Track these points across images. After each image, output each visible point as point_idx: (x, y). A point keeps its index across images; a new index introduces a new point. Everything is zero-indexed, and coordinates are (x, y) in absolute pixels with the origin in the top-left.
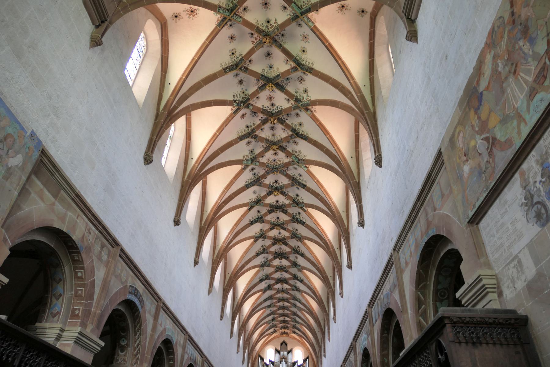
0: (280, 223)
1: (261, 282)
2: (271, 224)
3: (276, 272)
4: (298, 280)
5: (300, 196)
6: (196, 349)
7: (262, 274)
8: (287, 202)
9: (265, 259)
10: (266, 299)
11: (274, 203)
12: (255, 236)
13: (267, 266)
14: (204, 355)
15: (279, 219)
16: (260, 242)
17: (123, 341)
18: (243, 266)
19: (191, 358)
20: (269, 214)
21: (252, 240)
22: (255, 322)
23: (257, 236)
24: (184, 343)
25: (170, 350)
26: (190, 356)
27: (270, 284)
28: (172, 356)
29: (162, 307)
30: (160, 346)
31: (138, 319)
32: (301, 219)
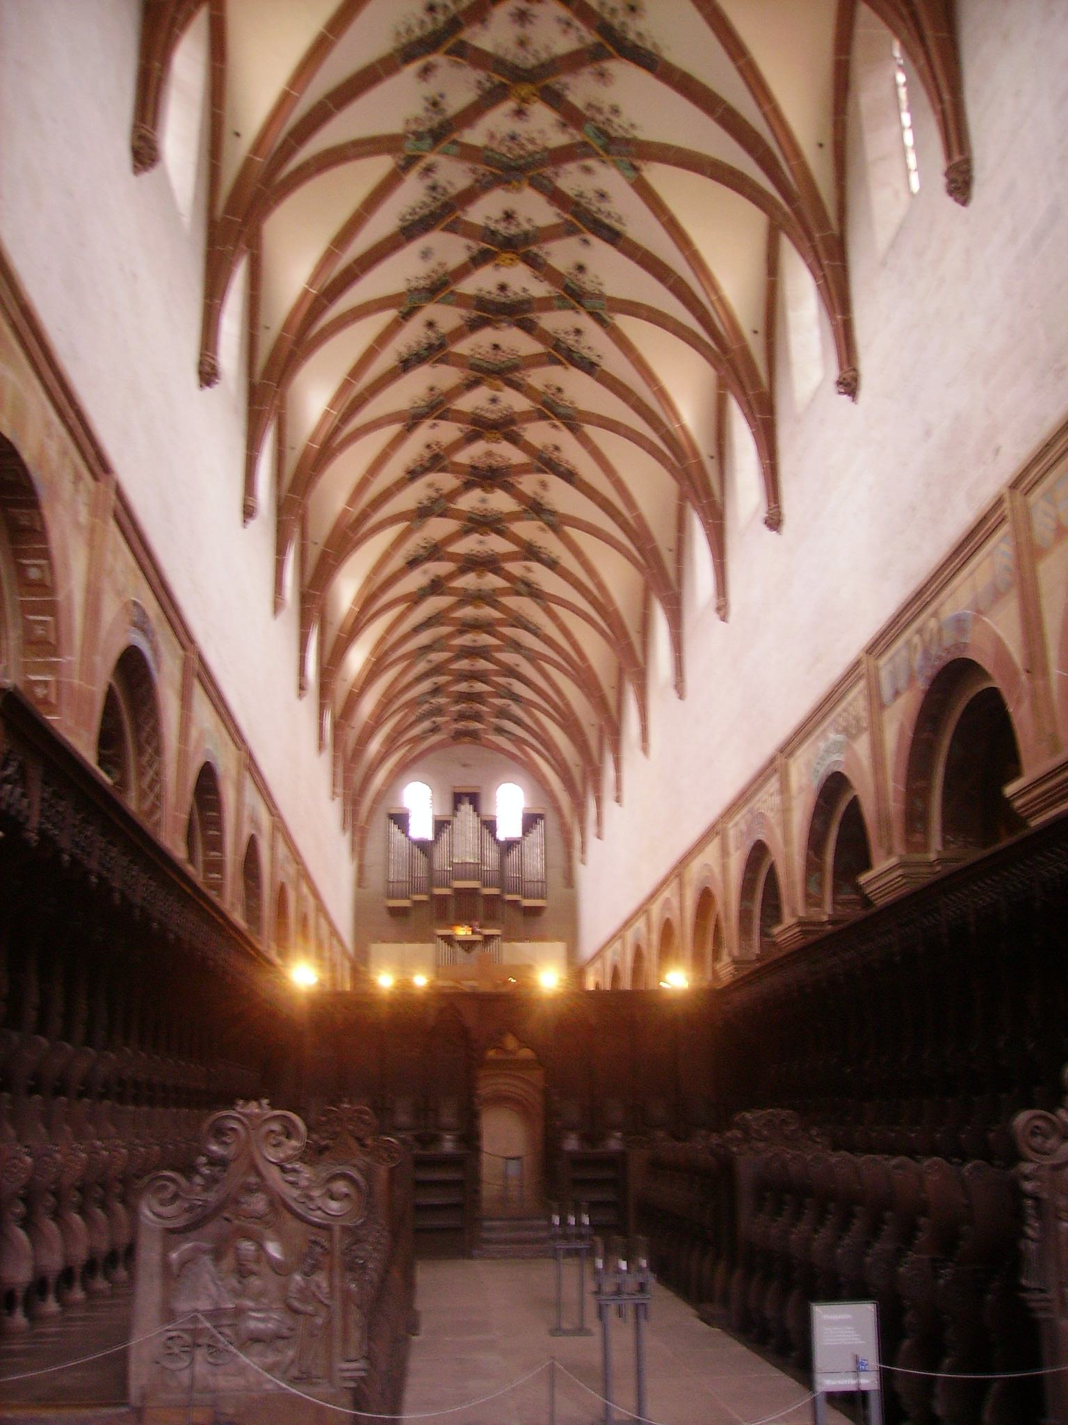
2: (474, 367)
4: (540, 560)
5: (593, 268)
7: (413, 545)
8: (540, 289)
16: (424, 434)
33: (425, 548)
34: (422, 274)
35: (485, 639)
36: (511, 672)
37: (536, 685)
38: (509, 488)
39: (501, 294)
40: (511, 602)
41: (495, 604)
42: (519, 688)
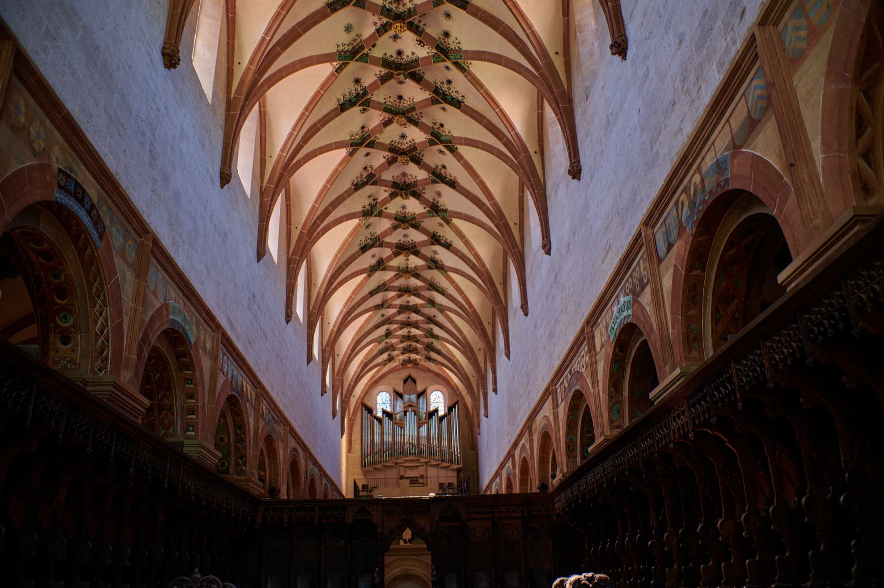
0: (405, 109)
1: (363, 253)
2: (386, 110)
3: (395, 228)
5: (454, 34)
6: (241, 368)
8: (423, 52)
9: (372, 199)
10: (374, 290)
11: (391, 56)
12: (352, 141)
13: (375, 216)
14: (259, 383)
15: (402, 101)
17: (65, 317)
18: (326, 213)
20: (382, 84)
21: (343, 152)
22: (353, 339)
23: (354, 141)
24: (213, 348)
26: (230, 379)
27: (381, 259)
29: (152, 251)
30: (157, 345)
32: (454, 95)
33: (371, 239)
34: (347, 42)
35: (415, 300)
36: (431, 320)
37: (446, 328)
38: (417, 195)
39: (399, 57)
40: (429, 274)
41: (417, 276)
42: (437, 331)
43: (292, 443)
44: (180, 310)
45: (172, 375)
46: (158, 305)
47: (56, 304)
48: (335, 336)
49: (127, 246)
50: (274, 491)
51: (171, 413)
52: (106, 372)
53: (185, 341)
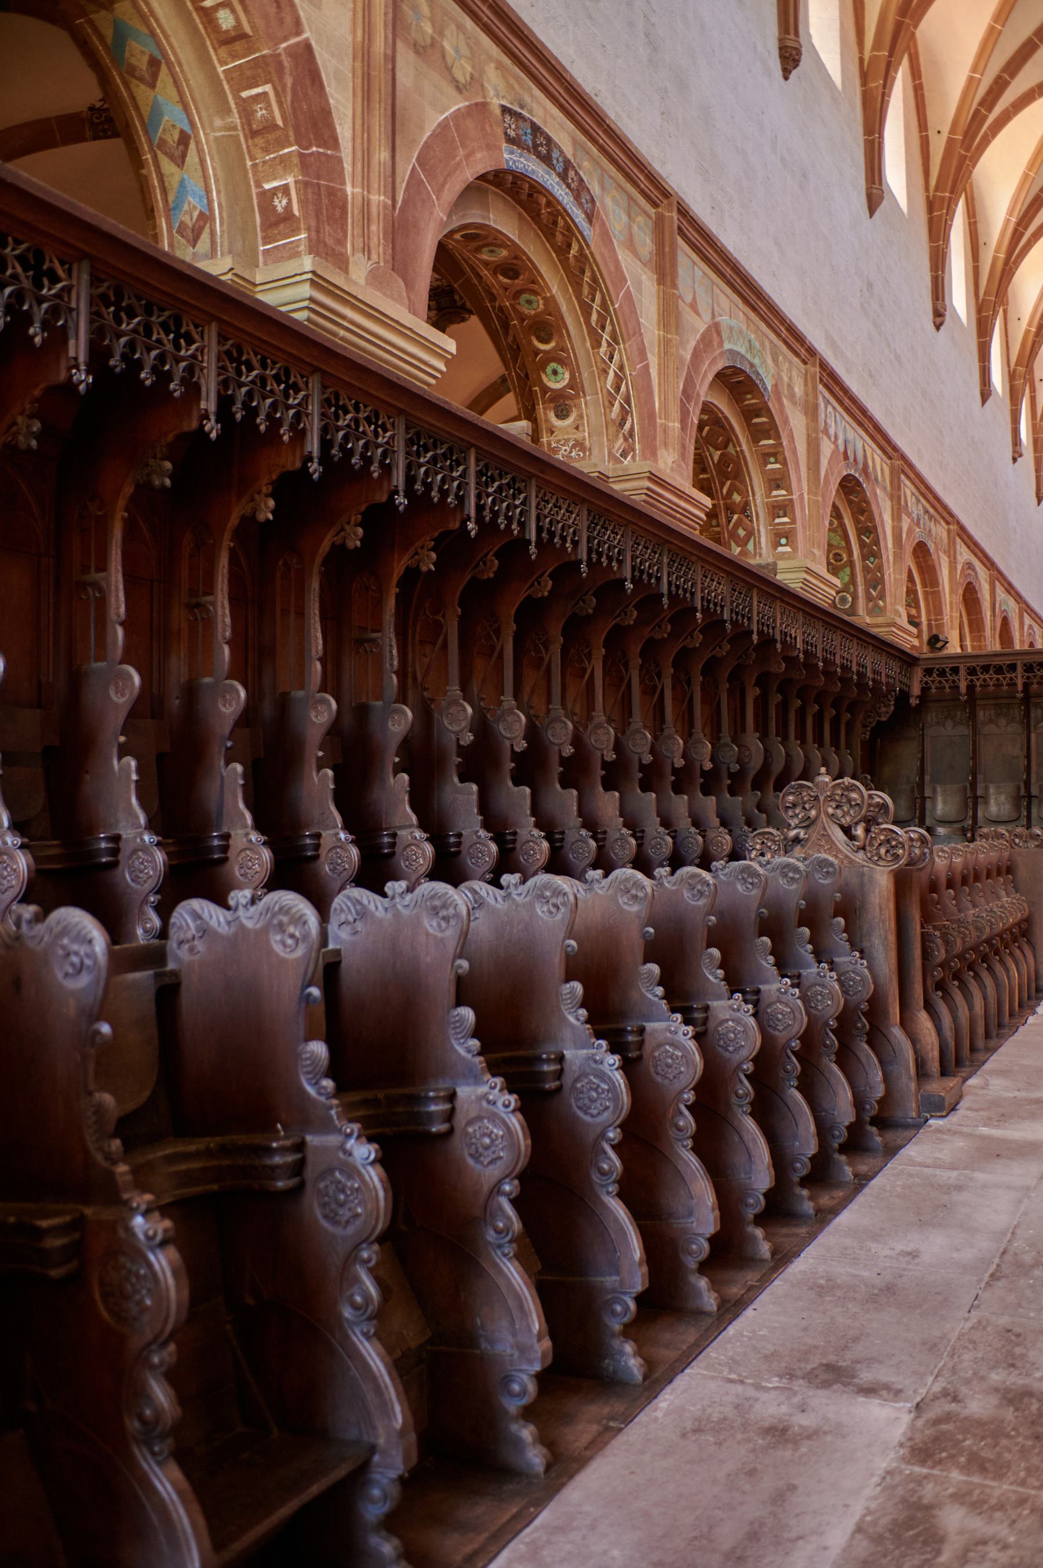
6: (860, 424)
14: (895, 449)
17: (555, 372)
19: (846, 457)
24: (807, 395)
25: (756, 420)
26: (842, 449)
28: (771, 442)
29: (679, 228)
30: (709, 399)
31: (588, 273)
43: (964, 554)
44: (741, 332)
45: (742, 451)
46: (702, 328)
47: (537, 352)
48: (1034, 342)
49: (635, 228)
50: (935, 641)
51: (747, 517)
52: (633, 457)
53: (757, 385)
